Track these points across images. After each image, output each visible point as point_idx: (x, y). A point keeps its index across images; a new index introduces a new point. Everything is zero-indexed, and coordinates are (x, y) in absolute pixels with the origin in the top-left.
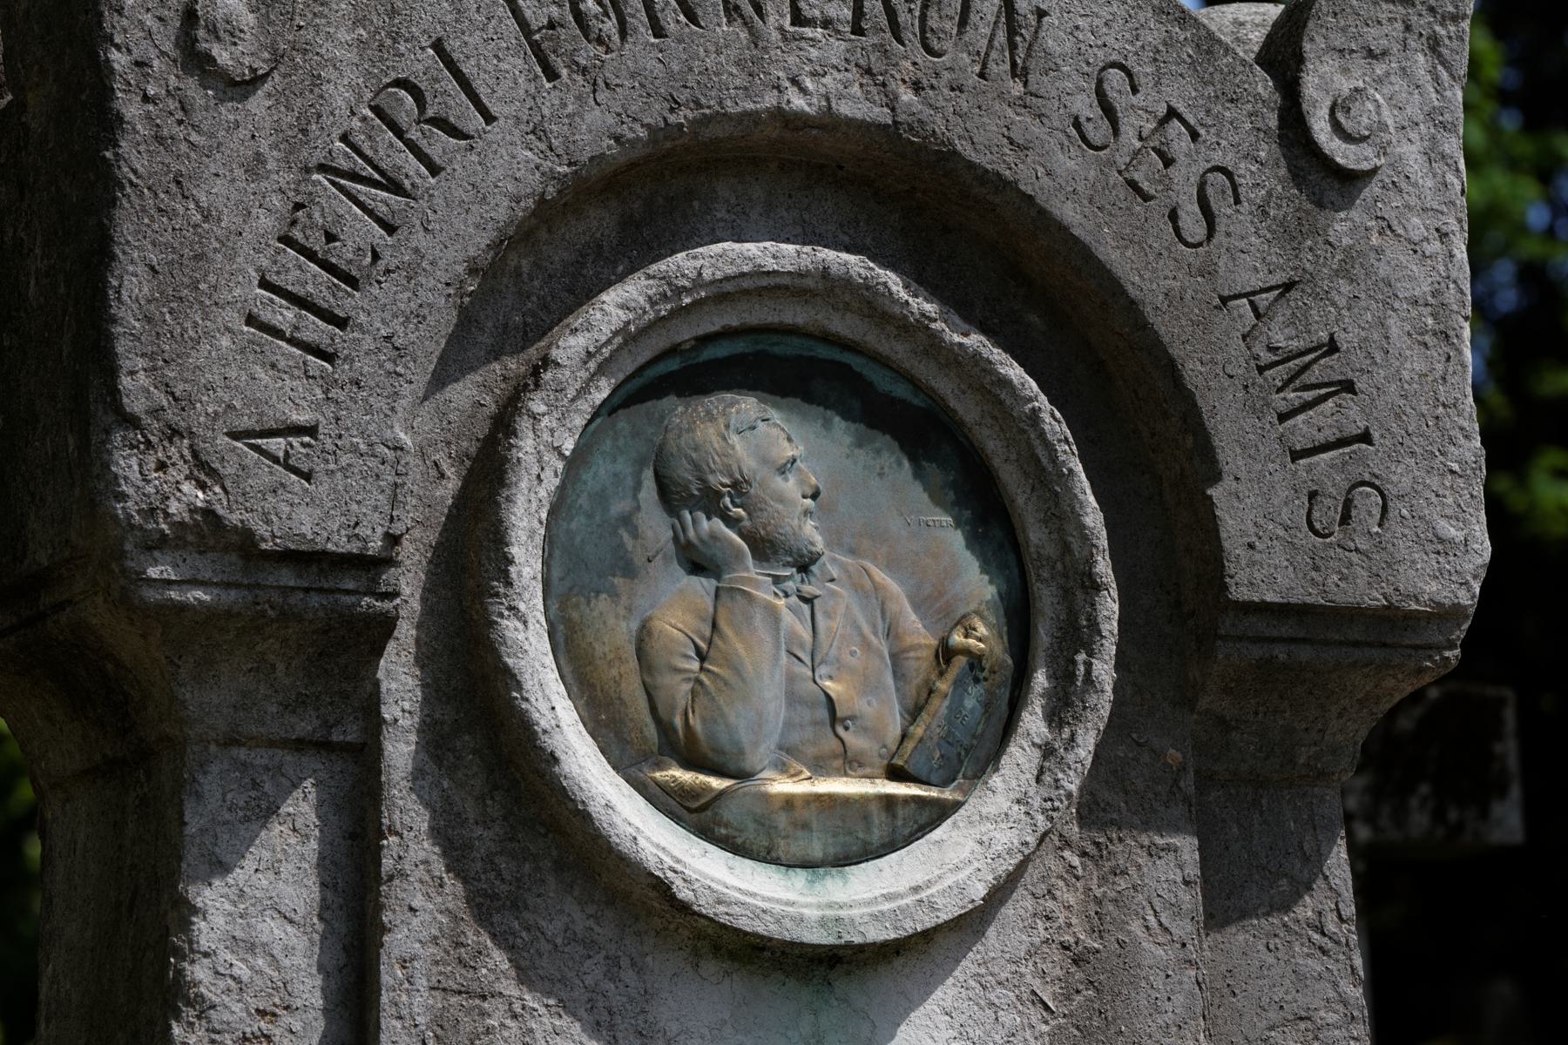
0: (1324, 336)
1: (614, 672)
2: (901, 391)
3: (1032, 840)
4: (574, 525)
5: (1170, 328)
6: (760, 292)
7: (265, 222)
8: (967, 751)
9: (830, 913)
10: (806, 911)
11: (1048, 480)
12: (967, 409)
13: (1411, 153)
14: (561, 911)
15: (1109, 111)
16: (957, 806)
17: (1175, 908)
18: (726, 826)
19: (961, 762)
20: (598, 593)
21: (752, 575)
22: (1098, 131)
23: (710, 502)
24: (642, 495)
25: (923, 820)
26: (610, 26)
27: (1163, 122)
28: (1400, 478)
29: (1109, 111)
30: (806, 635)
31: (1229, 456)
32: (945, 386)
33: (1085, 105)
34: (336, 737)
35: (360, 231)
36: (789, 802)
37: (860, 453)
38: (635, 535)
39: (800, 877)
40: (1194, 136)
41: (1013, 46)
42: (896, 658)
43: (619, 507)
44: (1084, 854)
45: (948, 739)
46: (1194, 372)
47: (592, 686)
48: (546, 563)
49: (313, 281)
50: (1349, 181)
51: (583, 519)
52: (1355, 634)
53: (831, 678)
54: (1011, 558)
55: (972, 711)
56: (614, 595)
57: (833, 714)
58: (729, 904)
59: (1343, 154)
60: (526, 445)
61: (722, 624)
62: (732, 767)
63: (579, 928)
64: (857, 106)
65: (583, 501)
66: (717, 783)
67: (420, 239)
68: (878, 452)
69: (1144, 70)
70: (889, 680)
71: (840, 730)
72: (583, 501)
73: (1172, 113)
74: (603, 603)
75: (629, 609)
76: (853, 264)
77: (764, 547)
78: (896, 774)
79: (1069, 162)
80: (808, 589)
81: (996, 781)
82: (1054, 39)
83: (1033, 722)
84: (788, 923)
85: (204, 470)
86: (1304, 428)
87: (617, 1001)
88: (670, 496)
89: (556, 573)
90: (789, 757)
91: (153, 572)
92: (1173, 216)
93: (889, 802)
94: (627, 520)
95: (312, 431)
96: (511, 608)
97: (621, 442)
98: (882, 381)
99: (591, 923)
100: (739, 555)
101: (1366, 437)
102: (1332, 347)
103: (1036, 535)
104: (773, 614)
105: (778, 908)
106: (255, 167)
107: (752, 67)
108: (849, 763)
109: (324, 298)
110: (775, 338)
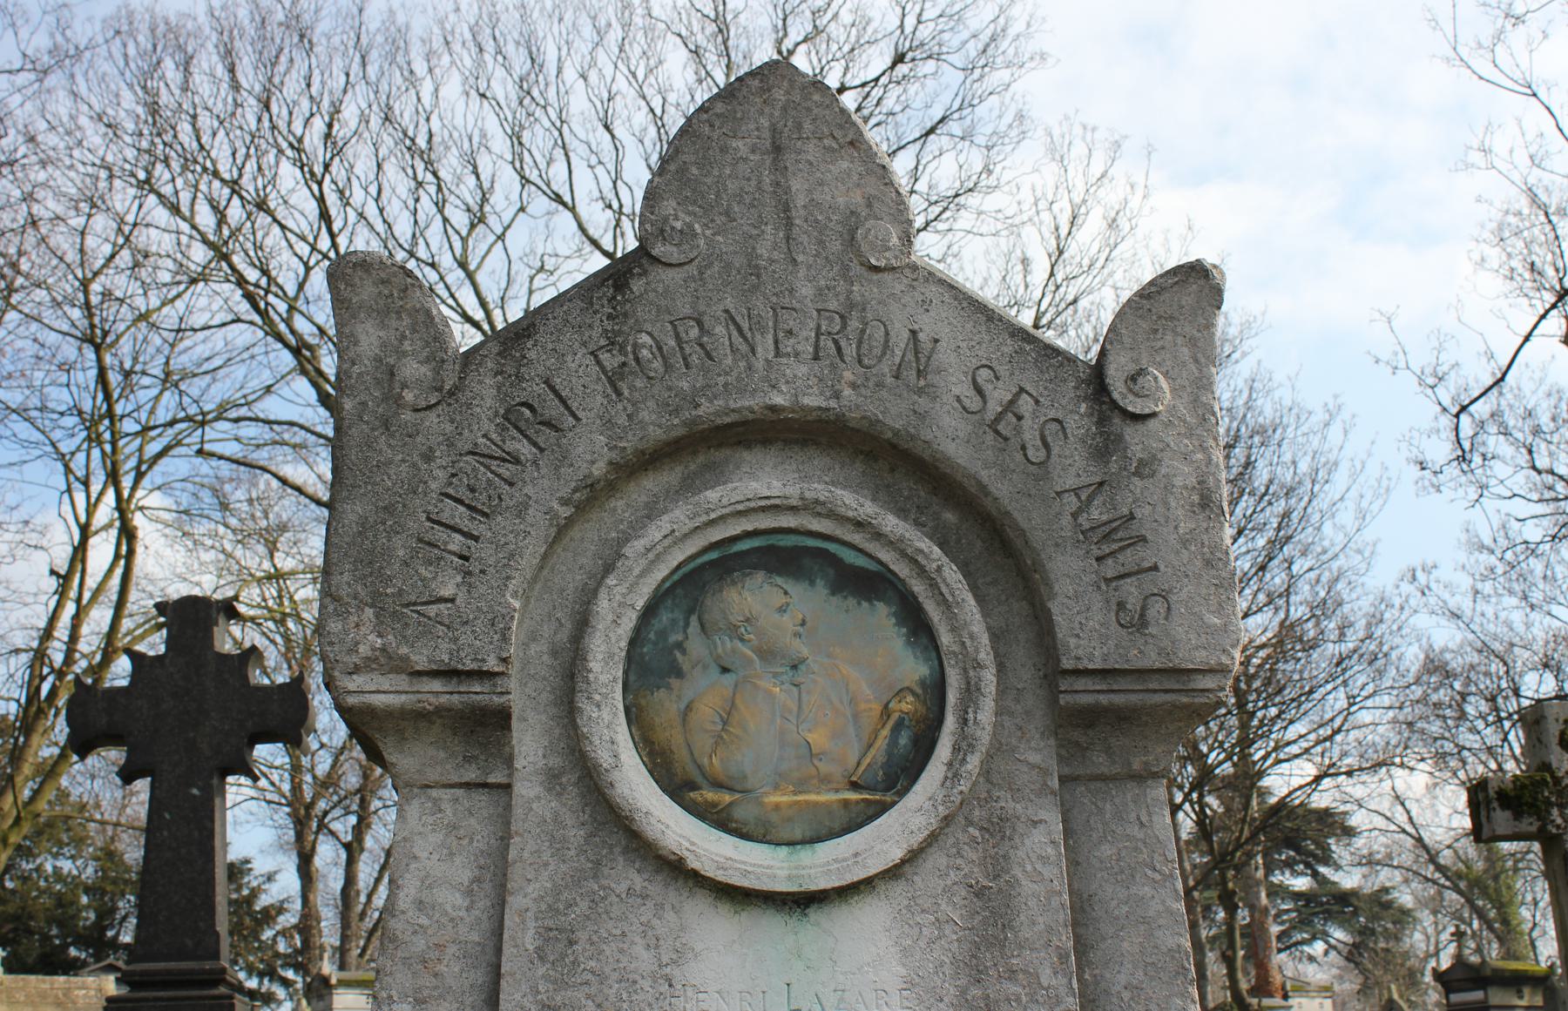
0: (1125, 511)
1: (667, 734)
2: (861, 561)
3: (934, 823)
4: (645, 650)
6: (763, 509)
8: (902, 771)
9: (794, 872)
10: (779, 872)
12: (902, 569)
14: (627, 878)
15: (979, 391)
16: (894, 804)
17: (1044, 859)
18: (736, 822)
19: (898, 778)
20: (659, 688)
22: (974, 403)
23: (733, 631)
24: (690, 630)
25: (871, 812)
26: (657, 364)
29: (979, 391)
30: (794, 707)
32: (886, 556)
33: (966, 390)
34: (491, 780)
36: (777, 807)
37: (835, 600)
38: (684, 652)
40: (1037, 402)
41: (918, 359)
42: (856, 716)
43: (675, 637)
44: (982, 829)
45: (887, 765)
47: (653, 743)
48: (626, 673)
49: (459, 515)
51: (650, 646)
53: (809, 731)
54: (934, 654)
55: (905, 746)
56: (669, 687)
58: (726, 869)
60: (603, 605)
61: (738, 702)
62: (738, 787)
63: (638, 888)
65: (652, 636)
66: (727, 798)
67: (529, 490)
68: (845, 598)
69: (1003, 370)
70: (851, 730)
71: (816, 762)
72: (652, 636)
73: (1022, 390)
74: (661, 694)
75: (679, 697)
77: (767, 654)
78: (855, 786)
81: (917, 787)
82: (944, 355)
83: (943, 751)
84: (765, 879)
87: (661, 931)
89: (632, 678)
91: (352, 687)
92: (1023, 448)
93: (846, 803)
94: (679, 646)
95: (452, 600)
96: (588, 698)
97: (677, 601)
98: (849, 557)
99: (646, 884)
100: (751, 661)
101: (1155, 568)
102: (1132, 517)
103: (945, 639)
104: (769, 694)
105: (759, 870)
108: (825, 781)
109: (466, 524)
110: (780, 536)
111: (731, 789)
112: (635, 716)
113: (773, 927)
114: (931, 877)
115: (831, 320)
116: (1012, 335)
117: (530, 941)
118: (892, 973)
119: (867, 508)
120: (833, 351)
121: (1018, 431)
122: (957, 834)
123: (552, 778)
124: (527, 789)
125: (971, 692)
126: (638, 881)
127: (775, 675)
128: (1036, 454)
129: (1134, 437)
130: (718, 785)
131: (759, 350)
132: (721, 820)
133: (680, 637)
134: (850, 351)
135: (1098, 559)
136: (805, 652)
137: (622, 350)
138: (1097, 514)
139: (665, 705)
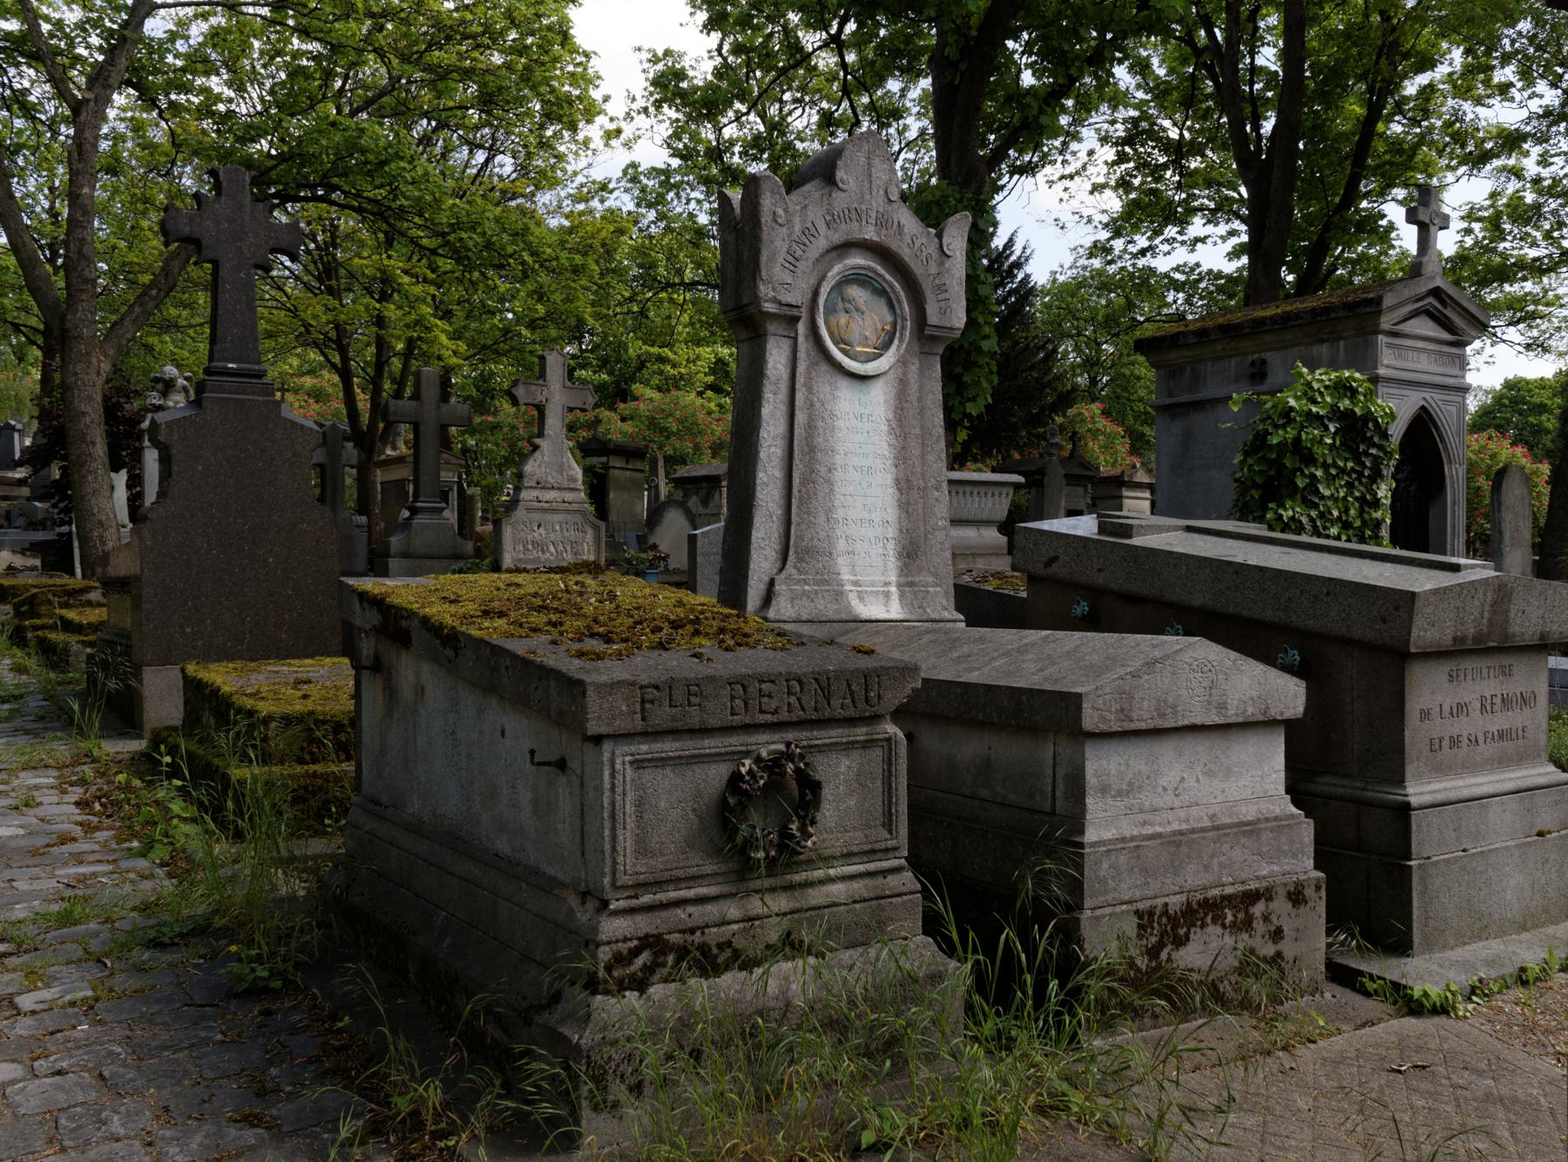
5: (921, 279)
7: (785, 249)
11: (899, 301)
12: (888, 290)
13: (958, 253)
21: (855, 314)
23: (849, 302)
28: (954, 306)
31: (929, 301)
32: (885, 285)
35: (799, 252)
46: (924, 286)
49: (791, 259)
50: (948, 257)
57: (866, 338)
59: (948, 252)
64: (875, 239)
76: (873, 264)
77: (857, 310)
79: (907, 250)
82: (906, 230)
83: (896, 341)
85: (774, 289)
86: (940, 297)
88: (843, 300)
90: (860, 344)
103: (898, 311)
106: (783, 240)
107: (860, 230)
108: (868, 346)
112: (826, 323)
113: (856, 384)
117: (802, 380)
118: (881, 399)
119: (883, 272)
123: (807, 337)
124: (801, 339)
125: (903, 328)
129: (947, 265)
138: (937, 282)
139: (833, 320)
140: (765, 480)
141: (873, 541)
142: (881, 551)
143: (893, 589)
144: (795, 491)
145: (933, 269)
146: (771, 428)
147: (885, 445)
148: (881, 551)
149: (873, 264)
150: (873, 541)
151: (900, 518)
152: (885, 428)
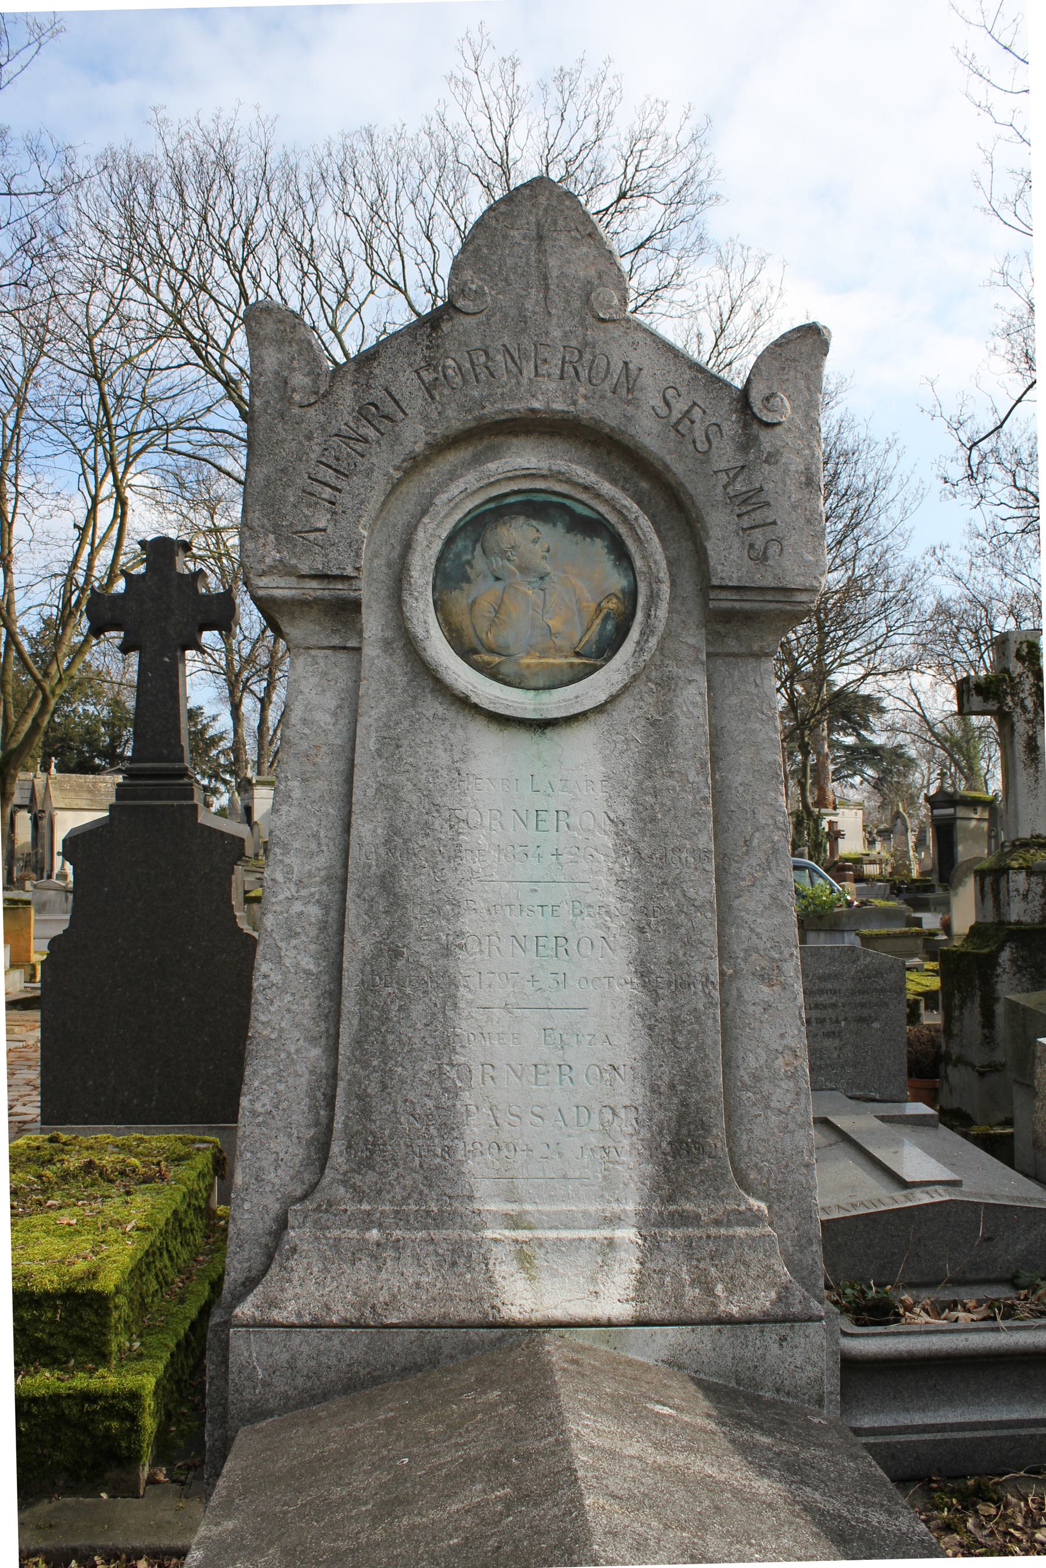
0: (757, 485)
2: (586, 512)
3: (627, 679)
6: (525, 476)
12: (612, 518)
15: (667, 404)
17: (695, 704)
22: (663, 411)
23: (503, 554)
26: (458, 380)
27: (691, 408)
29: (667, 404)
32: (603, 509)
33: (658, 403)
34: (349, 644)
36: (528, 666)
37: (569, 536)
38: (472, 567)
39: (531, 694)
40: (704, 412)
41: (628, 382)
42: (580, 611)
43: (466, 557)
44: (656, 684)
45: (598, 642)
48: (434, 579)
49: (329, 475)
52: (768, 598)
56: (461, 589)
60: (420, 535)
66: (497, 659)
67: (374, 460)
69: (683, 390)
73: (695, 404)
74: (456, 593)
78: (578, 654)
80: (544, 586)
81: (617, 656)
82: (646, 379)
83: (634, 634)
87: (454, 741)
89: (438, 582)
91: (261, 584)
92: (694, 442)
93: (572, 665)
94: (469, 563)
95: (324, 530)
98: (579, 509)
100: (514, 574)
101: (774, 523)
102: (761, 489)
103: (638, 563)
104: (525, 594)
108: (559, 651)
109: (333, 482)
111: (499, 654)
112: (439, 606)
113: (523, 740)
114: (622, 712)
115: (573, 353)
116: (690, 367)
117: (372, 744)
118: (597, 771)
120: (573, 374)
121: (691, 430)
122: (641, 686)
123: (387, 645)
124: (371, 651)
125: (653, 598)
126: (440, 710)
127: (530, 583)
128: (702, 446)
129: (766, 438)
130: (491, 651)
131: (525, 372)
132: (493, 673)
133: (469, 557)
134: (584, 374)
135: (739, 516)
136: (549, 569)
137: (435, 370)
138: (739, 486)
139: (459, 600)
140: (276, 978)
141: (571, 1114)
142: (593, 1140)
143: (627, 1234)
144: (349, 1004)
145: (725, 455)
146: (293, 860)
147: (606, 881)
148: (593, 1140)
149: (560, 465)
150: (571, 1114)
151: (647, 1058)
152: (609, 842)
